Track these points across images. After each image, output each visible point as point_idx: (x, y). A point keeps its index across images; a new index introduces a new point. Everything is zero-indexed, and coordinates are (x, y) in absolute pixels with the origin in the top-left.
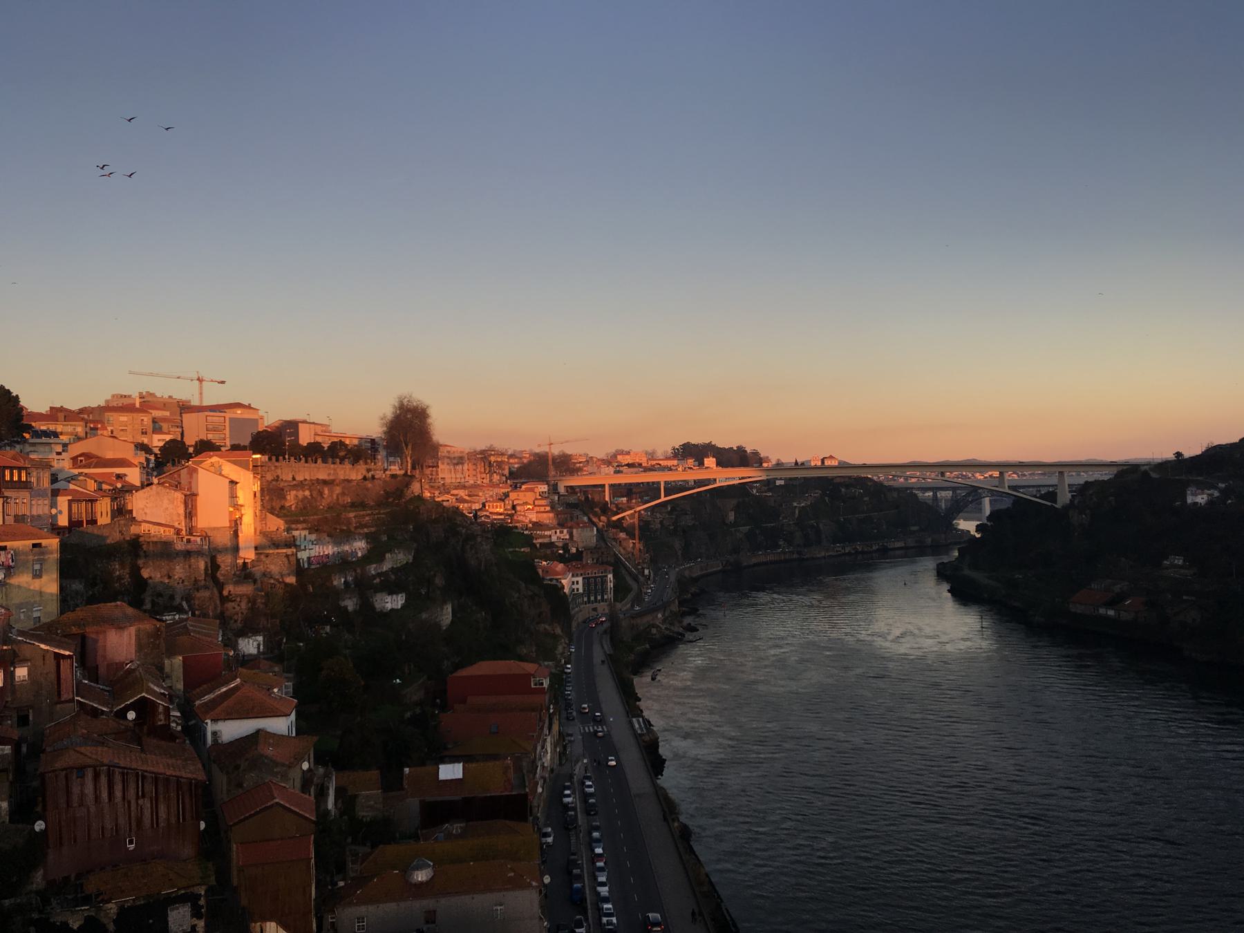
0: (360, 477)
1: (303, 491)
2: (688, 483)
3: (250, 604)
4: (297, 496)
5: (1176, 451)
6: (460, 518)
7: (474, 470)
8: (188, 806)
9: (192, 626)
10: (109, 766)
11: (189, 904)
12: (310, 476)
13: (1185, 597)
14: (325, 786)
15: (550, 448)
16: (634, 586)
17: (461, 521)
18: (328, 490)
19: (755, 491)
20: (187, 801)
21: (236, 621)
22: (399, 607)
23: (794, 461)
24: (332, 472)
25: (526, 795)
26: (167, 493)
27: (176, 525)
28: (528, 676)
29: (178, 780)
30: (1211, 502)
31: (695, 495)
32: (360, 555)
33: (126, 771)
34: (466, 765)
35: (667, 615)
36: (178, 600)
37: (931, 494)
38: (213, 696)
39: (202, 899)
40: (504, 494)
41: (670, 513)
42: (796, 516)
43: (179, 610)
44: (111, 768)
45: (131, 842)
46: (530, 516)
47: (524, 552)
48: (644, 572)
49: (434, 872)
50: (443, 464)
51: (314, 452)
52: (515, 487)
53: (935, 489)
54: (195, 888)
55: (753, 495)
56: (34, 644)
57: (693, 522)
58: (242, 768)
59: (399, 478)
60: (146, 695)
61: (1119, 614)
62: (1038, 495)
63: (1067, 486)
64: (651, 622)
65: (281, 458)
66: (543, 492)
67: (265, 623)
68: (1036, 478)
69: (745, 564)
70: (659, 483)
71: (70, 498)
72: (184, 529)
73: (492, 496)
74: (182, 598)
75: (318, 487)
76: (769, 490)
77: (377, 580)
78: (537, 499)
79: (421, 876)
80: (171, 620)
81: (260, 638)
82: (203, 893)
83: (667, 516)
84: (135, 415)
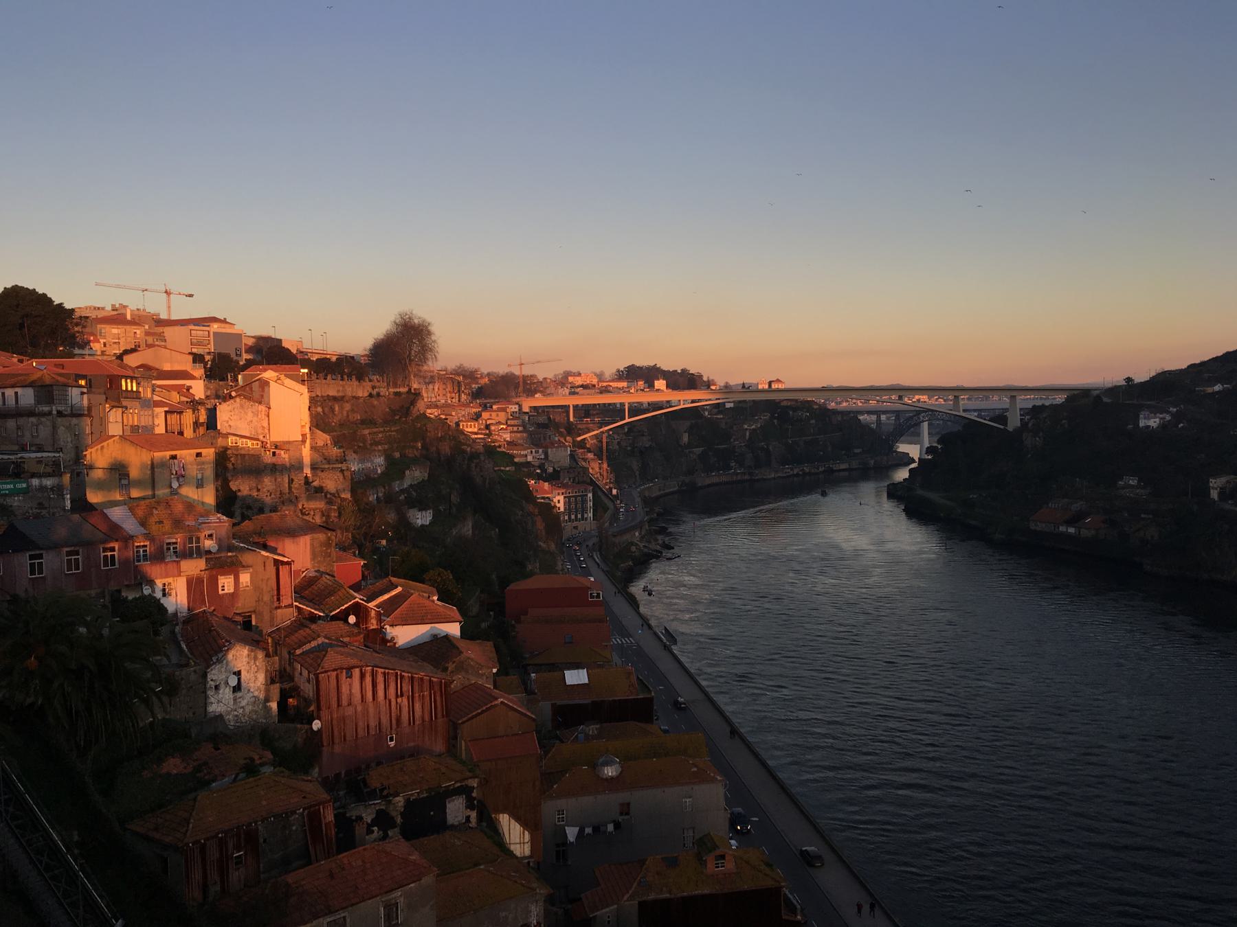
0: (366, 394)
2: (642, 404)
3: (324, 518)
6: (463, 436)
7: (444, 389)
11: (464, 796)
12: (321, 392)
13: (1143, 516)
15: (521, 369)
19: (707, 413)
20: (438, 699)
24: (341, 389)
25: (651, 700)
27: (261, 437)
30: (1164, 426)
32: (379, 471)
33: (387, 671)
35: (643, 533)
37: (874, 417)
40: (476, 413)
41: (627, 434)
42: (747, 438)
44: (375, 669)
45: (391, 739)
46: (505, 436)
48: (612, 491)
49: (622, 767)
52: (485, 407)
53: (877, 413)
54: (470, 780)
56: (255, 551)
57: (650, 443)
58: (450, 668)
59: (403, 396)
61: (1079, 532)
62: (988, 418)
63: (1018, 410)
67: (341, 537)
69: (700, 485)
71: (167, 409)
73: (464, 416)
75: (330, 404)
77: (402, 497)
78: (508, 419)
79: (610, 772)
82: (475, 785)
83: (624, 437)
84: (128, 327)
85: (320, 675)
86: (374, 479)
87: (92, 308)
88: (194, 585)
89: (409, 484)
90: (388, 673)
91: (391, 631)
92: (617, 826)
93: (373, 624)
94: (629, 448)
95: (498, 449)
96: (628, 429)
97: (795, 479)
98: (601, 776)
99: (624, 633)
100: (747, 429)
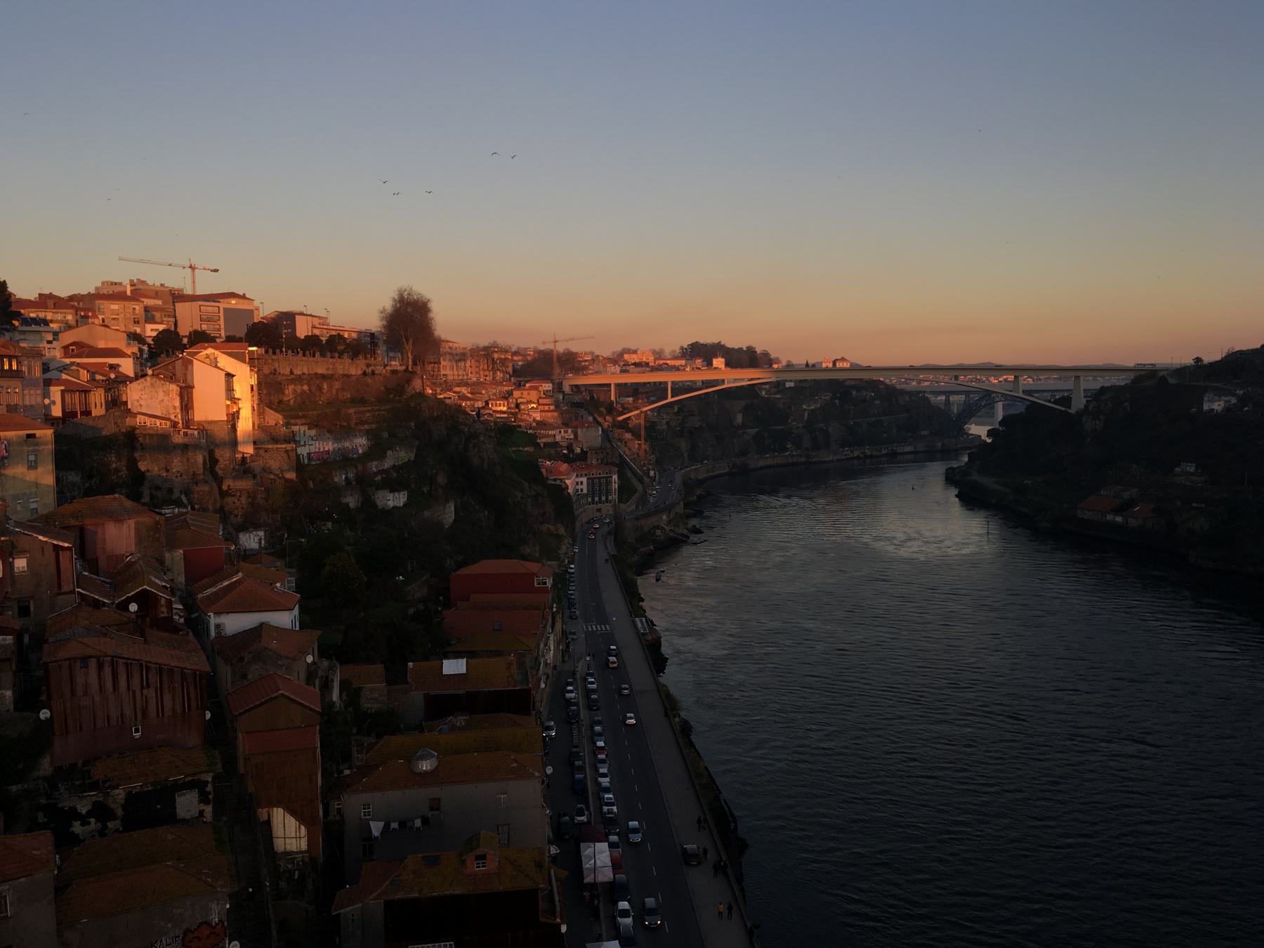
0: (360, 372)
1: (302, 385)
2: (696, 383)
4: (295, 391)
5: (1196, 357)
8: (192, 696)
9: (191, 519)
10: (113, 657)
11: (197, 790)
12: (308, 370)
13: (1194, 505)
14: (330, 679)
15: (555, 346)
16: (639, 487)
17: (463, 419)
18: (327, 385)
19: (764, 393)
20: (192, 689)
21: (236, 516)
22: (402, 505)
23: (805, 363)
24: (331, 367)
25: (528, 691)
26: (163, 384)
27: (172, 417)
28: (533, 575)
29: (182, 671)
30: (1228, 410)
31: (703, 396)
32: (360, 451)
33: (130, 661)
34: (470, 661)
35: (672, 516)
36: (176, 495)
37: (943, 398)
38: (215, 590)
39: (209, 785)
40: (508, 392)
41: (677, 414)
42: (806, 419)
43: (178, 503)
45: (137, 731)
46: (534, 415)
47: (527, 451)
48: (649, 472)
49: (439, 762)
50: (444, 360)
51: (311, 345)
52: (519, 386)
53: (948, 393)
55: (762, 397)
58: (246, 659)
59: (400, 374)
60: (148, 588)
62: (1052, 400)
64: (655, 524)
65: (278, 351)
66: (547, 391)
67: (266, 518)
68: (1052, 383)
69: (752, 466)
70: (666, 383)
71: (63, 388)
72: (181, 422)
73: (494, 394)
74: (181, 492)
75: (317, 382)
77: (379, 478)
78: (541, 398)
79: (426, 766)
80: (171, 513)
81: (261, 534)
82: (210, 780)
85: (50, 664)
86: (353, 459)
87: (109, 284)
89: (392, 464)
90: (131, 663)
92: (425, 821)
94: (678, 429)
95: (518, 429)
96: (678, 409)
97: (856, 462)
98: (415, 770)
99: (603, 618)
100: (805, 409)
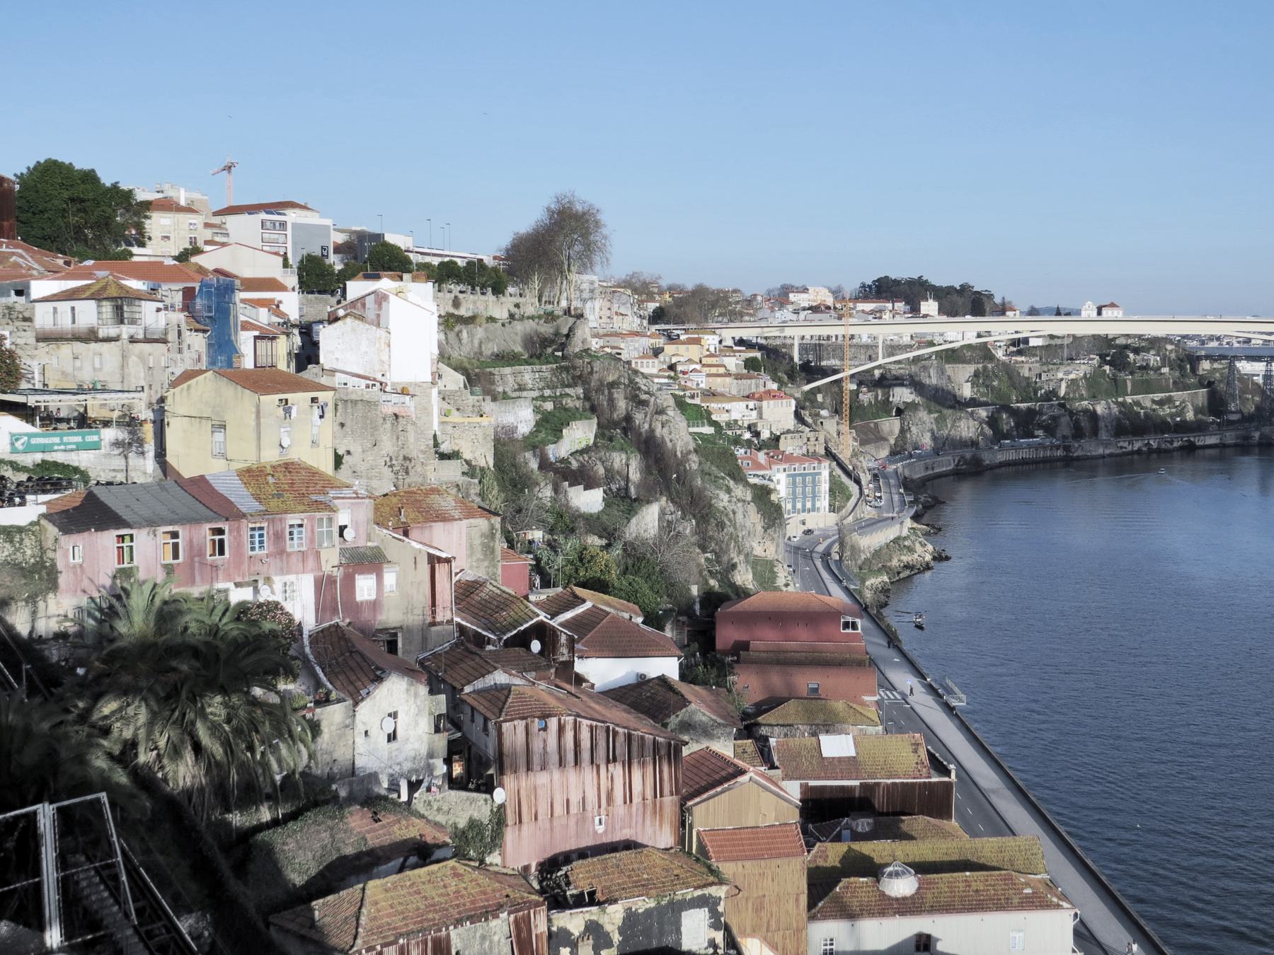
27: (379, 377)
44: (578, 719)
71: (257, 333)
76: (1020, 353)
82: (723, 896)
88: (323, 585)
90: (596, 726)
91: (581, 667)
93: (564, 651)
100: (1062, 380)
